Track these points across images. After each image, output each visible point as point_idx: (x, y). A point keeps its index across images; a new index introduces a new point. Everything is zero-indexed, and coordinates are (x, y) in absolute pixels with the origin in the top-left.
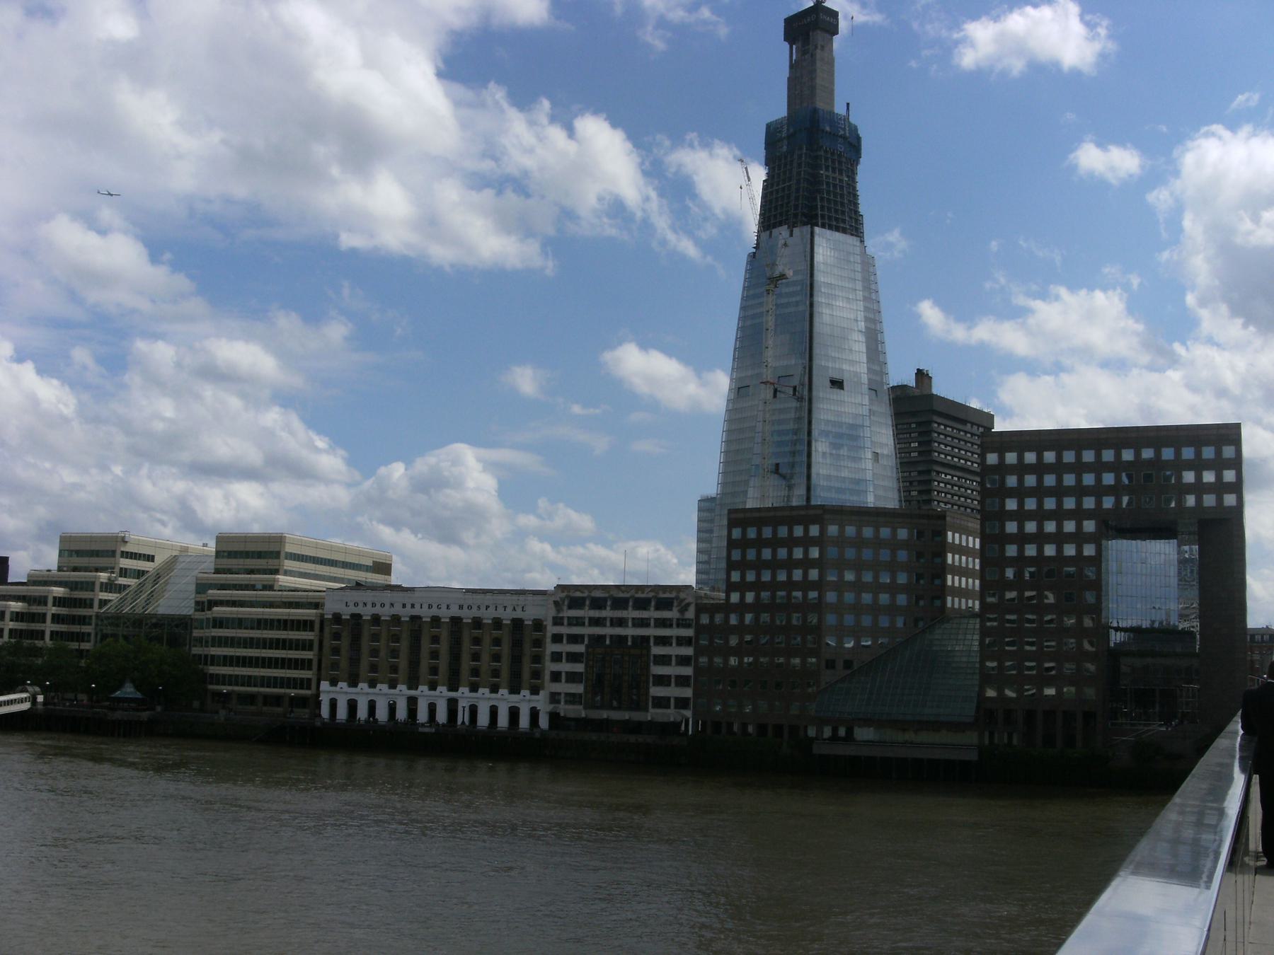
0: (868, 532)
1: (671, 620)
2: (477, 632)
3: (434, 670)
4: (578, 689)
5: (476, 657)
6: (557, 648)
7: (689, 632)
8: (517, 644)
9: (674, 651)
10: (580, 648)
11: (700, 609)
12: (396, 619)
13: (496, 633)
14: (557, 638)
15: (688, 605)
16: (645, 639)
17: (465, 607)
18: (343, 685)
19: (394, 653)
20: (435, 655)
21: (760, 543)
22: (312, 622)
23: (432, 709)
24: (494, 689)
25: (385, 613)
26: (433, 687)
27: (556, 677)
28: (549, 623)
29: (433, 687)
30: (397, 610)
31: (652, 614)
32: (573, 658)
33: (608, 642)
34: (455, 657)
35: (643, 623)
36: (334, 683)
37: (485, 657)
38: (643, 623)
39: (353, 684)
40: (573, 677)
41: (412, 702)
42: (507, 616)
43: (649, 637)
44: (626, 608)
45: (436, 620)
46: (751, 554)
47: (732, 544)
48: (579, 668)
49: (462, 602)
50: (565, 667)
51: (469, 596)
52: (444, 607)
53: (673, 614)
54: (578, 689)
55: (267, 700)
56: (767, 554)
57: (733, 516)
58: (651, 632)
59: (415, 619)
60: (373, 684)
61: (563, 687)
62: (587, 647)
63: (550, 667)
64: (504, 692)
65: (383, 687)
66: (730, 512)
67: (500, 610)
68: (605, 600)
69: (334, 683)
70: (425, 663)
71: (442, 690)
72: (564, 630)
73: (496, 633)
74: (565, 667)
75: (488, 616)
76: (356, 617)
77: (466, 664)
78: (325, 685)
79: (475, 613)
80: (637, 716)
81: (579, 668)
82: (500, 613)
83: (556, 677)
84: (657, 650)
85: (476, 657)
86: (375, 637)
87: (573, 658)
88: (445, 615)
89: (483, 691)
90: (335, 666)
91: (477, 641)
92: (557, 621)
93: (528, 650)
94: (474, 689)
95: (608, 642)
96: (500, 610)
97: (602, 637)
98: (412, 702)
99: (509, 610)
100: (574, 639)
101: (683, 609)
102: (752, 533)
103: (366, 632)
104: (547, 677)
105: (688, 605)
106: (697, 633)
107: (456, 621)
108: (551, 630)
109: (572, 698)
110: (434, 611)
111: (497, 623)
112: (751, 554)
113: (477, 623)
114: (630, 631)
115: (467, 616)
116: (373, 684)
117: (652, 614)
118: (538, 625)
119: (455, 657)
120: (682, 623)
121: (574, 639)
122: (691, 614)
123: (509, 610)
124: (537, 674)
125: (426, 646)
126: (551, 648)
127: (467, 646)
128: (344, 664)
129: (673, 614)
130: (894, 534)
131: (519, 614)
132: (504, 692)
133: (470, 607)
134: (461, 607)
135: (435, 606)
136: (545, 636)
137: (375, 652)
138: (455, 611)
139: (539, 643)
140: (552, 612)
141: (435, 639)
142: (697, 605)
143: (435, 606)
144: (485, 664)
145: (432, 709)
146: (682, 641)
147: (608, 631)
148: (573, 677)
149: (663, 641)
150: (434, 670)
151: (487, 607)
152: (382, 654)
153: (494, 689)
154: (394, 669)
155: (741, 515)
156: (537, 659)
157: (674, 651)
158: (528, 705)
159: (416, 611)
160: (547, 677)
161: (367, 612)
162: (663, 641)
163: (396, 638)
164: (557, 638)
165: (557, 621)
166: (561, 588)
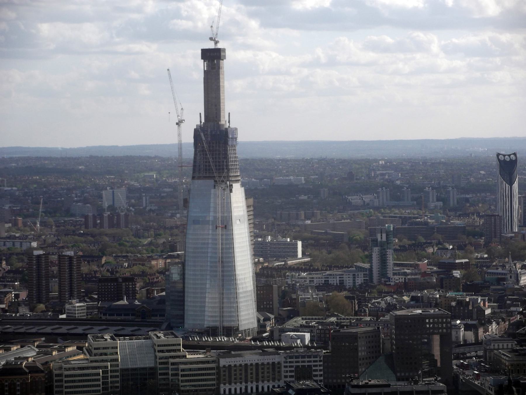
3: (252, 378)
5: (263, 373)
7: (321, 363)
8: (273, 369)
9: (318, 368)
10: (293, 369)
12: (241, 365)
13: (268, 366)
18: (227, 385)
19: (241, 374)
20: (251, 374)
22: (214, 368)
23: (252, 388)
24: (268, 381)
25: (238, 364)
26: (252, 382)
27: (286, 377)
29: (252, 382)
30: (241, 362)
31: (312, 359)
32: (291, 371)
34: (257, 374)
36: (225, 384)
37: (266, 373)
39: (230, 384)
41: (246, 388)
42: (271, 362)
45: (251, 365)
48: (293, 374)
53: (318, 359)
55: (201, 390)
59: (246, 365)
60: (236, 383)
61: (288, 379)
63: (283, 374)
64: (271, 382)
65: (238, 384)
68: (299, 356)
69: (225, 384)
70: (249, 376)
71: (255, 383)
72: (288, 364)
76: (230, 366)
77: (260, 375)
78: (222, 385)
81: (293, 374)
82: (269, 361)
83: (286, 377)
84: (314, 368)
85: (263, 373)
86: (235, 371)
87: (291, 371)
88: (254, 363)
89: (266, 382)
90: (225, 380)
91: (263, 369)
93: (277, 370)
94: (263, 381)
97: (299, 366)
98: (246, 388)
101: (320, 358)
103: (233, 369)
104: (283, 377)
107: (257, 364)
108: (283, 364)
110: (251, 362)
113: (263, 364)
114: (306, 364)
115: (260, 362)
116: (236, 383)
117: (312, 359)
118: (279, 363)
119: (257, 374)
120: (320, 361)
122: (322, 359)
124: (280, 376)
125: (249, 371)
126: (283, 369)
127: (260, 371)
128: (227, 379)
129: (318, 359)
131: (274, 361)
132: (271, 382)
136: (281, 366)
137: (235, 375)
138: (257, 362)
139: (279, 368)
140: (284, 360)
141: (251, 369)
144: (266, 374)
145: (252, 388)
149: (316, 366)
150: (252, 378)
152: (238, 375)
153: (268, 381)
154: (241, 379)
156: (279, 372)
157: (318, 368)
159: (246, 362)
160: (283, 377)
161: (233, 364)
162: (316, 366)
163: (241, 370)
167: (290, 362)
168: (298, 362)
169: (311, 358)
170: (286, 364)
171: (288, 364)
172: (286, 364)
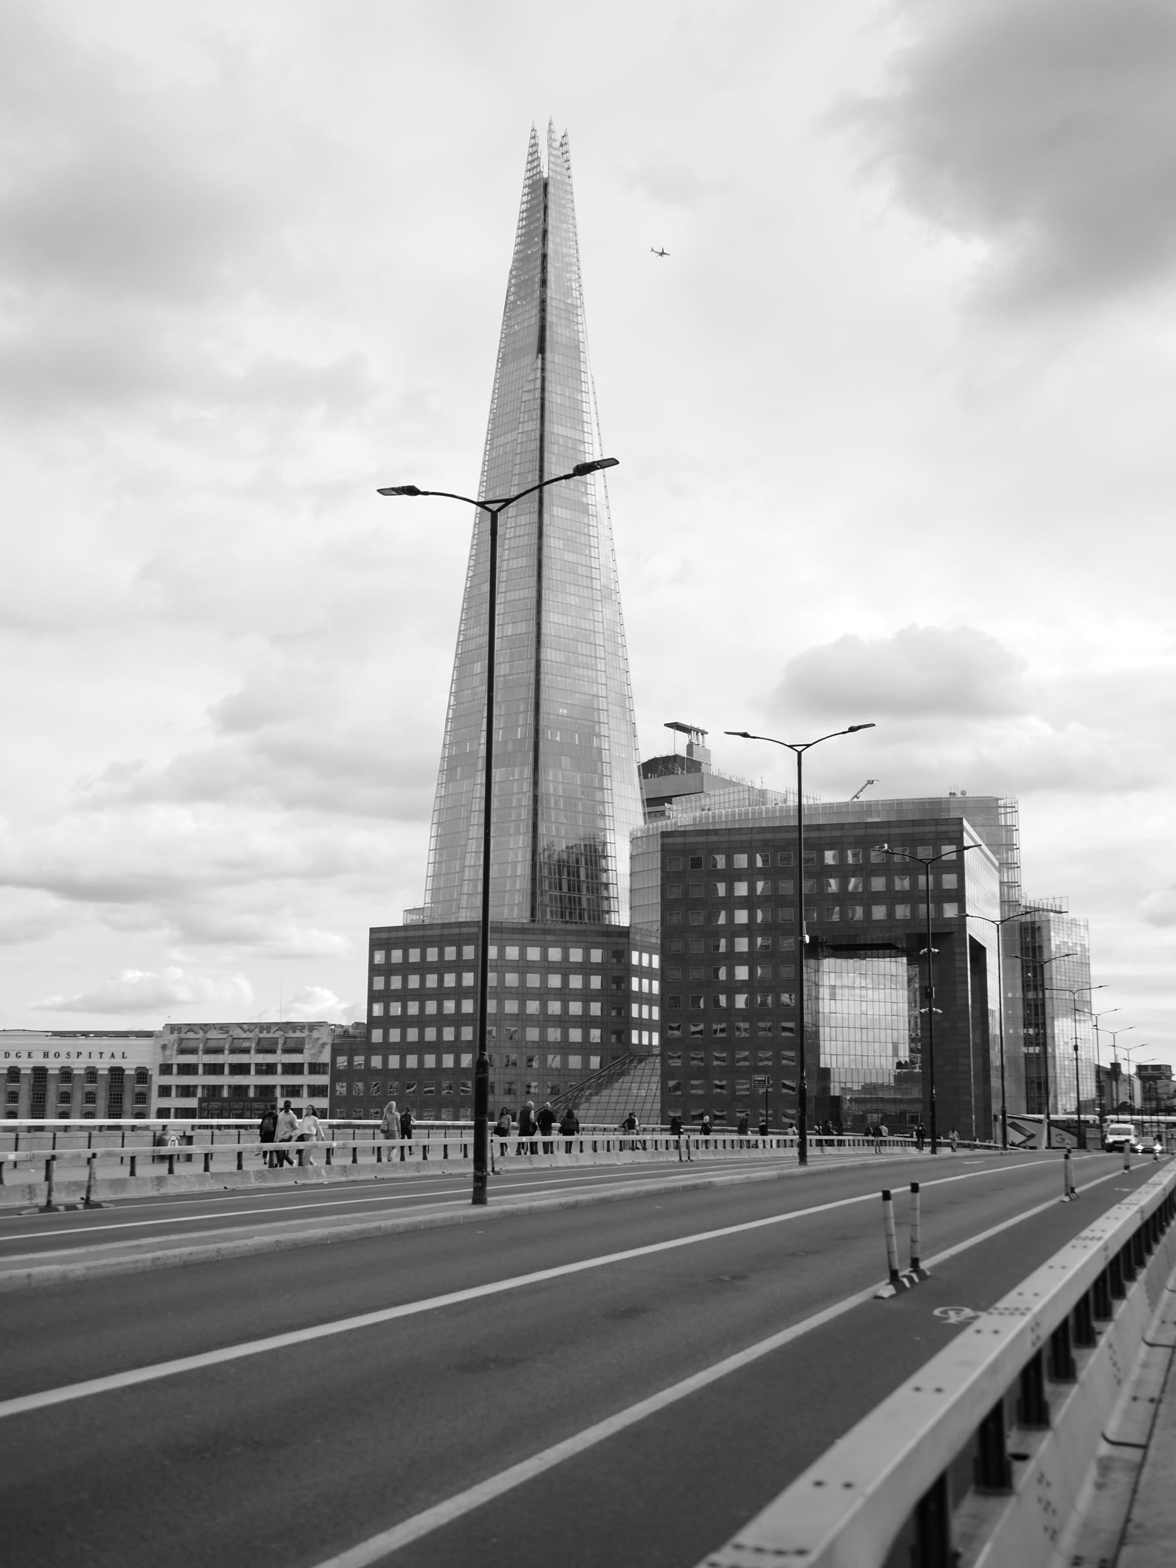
0: (534, 954)
1: (302, 1065)
2: (65, 1087)
6: (165, 1103)
7: (323, 1080)
11: (336, 1051)
13: (90, 1087)
14: (165, 1091)
15: (324, 1045)
16: (270, 1089)
17: (51, 1055)
21: (406, 968)
28: (154, 1072)
33: (225, 1094)
35: (270, 1069)
38: (270, 1069)
42: (104, 1066)
43: (274, 1087)
44: (246, 1051)
46: (396, 983)
47: (374, 970)
49: (46, 1049)
51: (58, 1041)
52: (24, 1055)
56: (414, 982)
57: (376, 936)
58: (279, 1080)
62: (201, 1100)
66: (372, 930)
67: (95, 1056)
72: (174, 1080)
73: (90, 1087)
75: (79, 1066)
79: (63, 1061)
88: (25, 1065)
92: (166, 1069)
95: (225, 1094)
96: (95, 1056)
99: (106, 1056)
100: (186, 1091)
102: (397, 956)
105: (324, 1045)
106: (334, 1081)
107: (40, 1073)
108: (158, 1080)
111: (91, 1074)
112: (396, 983)
113: (66, 1074)
114: (252, 1080)
115: (53, 1066)
118: (142, 1075)
120: (315, 1069)
121: (186, 1091)
122: (325, 1058)
123: (106, 1056)
130: (566, 956)
131: (117, 1062)
133: (57, 1055)
134: (46, 1055)
135: (13, 1054)
136: (149, 1088)
138: (38, 1061)
139: (142, 1098)
142: (333, 1045)
143: (13, 1054)
146: (316, 1091)
147: (226, 1080)
149: (294, 1091)
151: (79, 1054)
155: (384, 935)
164: (165, 1091)
165: (166, 1069)
166: (173, 1028)
168: (215, 1069)
169: (273, 1051)
170: (167, 1080)
171: (174, 1080)
172: (167, 1080)
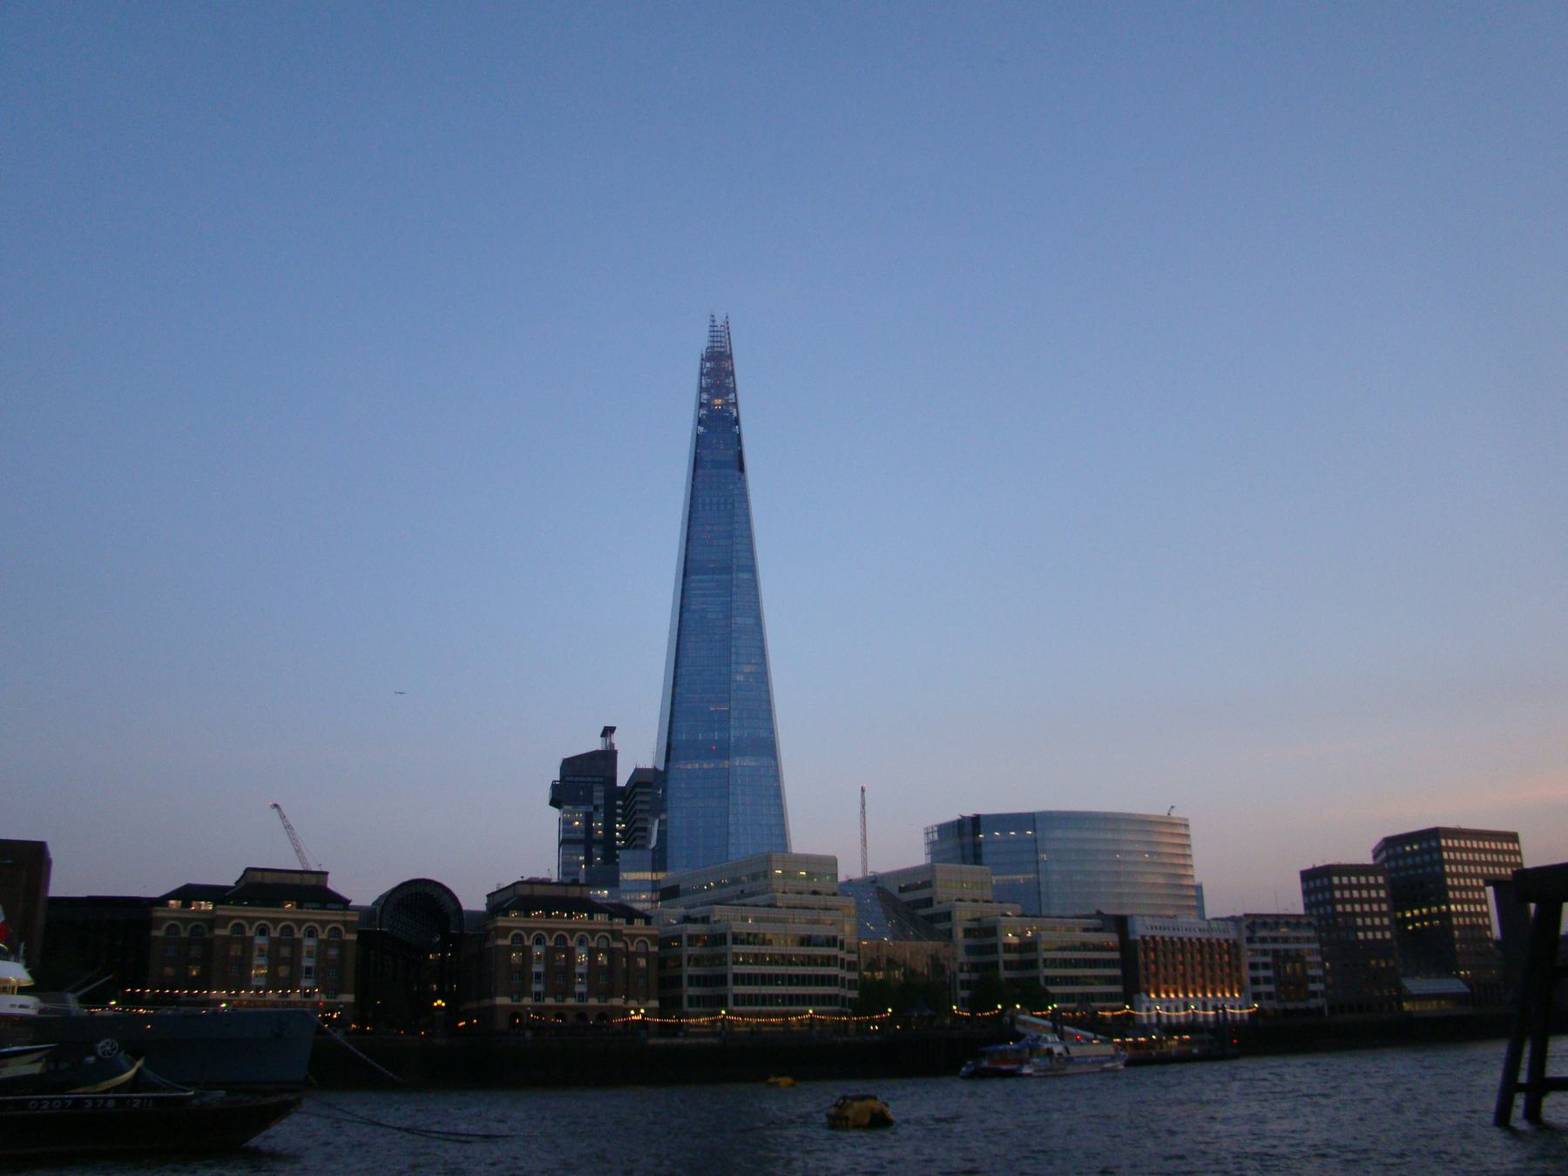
4: (1271, 988)
27: (1255, 981)
40: (1267, 980)
48: (1270, 973)
50: (1262, 973)
54: (1271, 988)
74: (1262, 973)
80: (1301, 1005)
83: (1255, 981)
100: (1265, 953)
109: (1269, 996)
121: (1265, 953)
140: (1246, 933)
148: (1267, 980)
158: (1237, 1006)
165: (1250, 940)
167: (1263, 940)
